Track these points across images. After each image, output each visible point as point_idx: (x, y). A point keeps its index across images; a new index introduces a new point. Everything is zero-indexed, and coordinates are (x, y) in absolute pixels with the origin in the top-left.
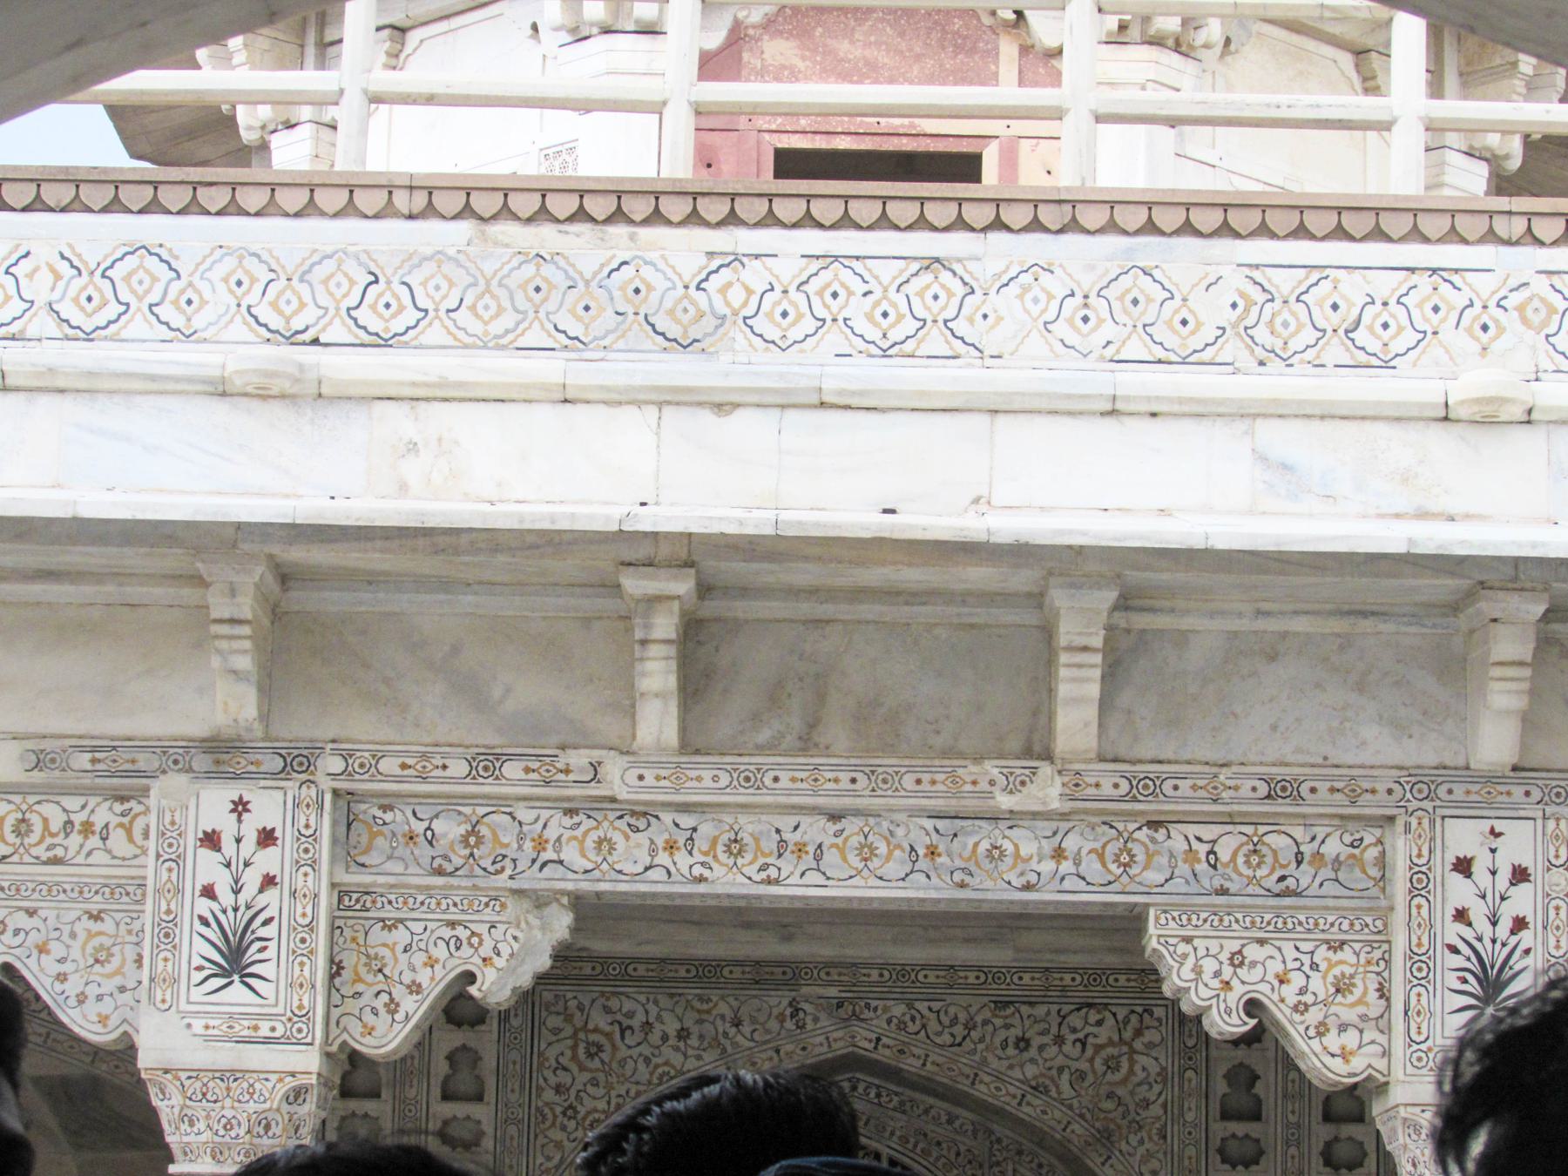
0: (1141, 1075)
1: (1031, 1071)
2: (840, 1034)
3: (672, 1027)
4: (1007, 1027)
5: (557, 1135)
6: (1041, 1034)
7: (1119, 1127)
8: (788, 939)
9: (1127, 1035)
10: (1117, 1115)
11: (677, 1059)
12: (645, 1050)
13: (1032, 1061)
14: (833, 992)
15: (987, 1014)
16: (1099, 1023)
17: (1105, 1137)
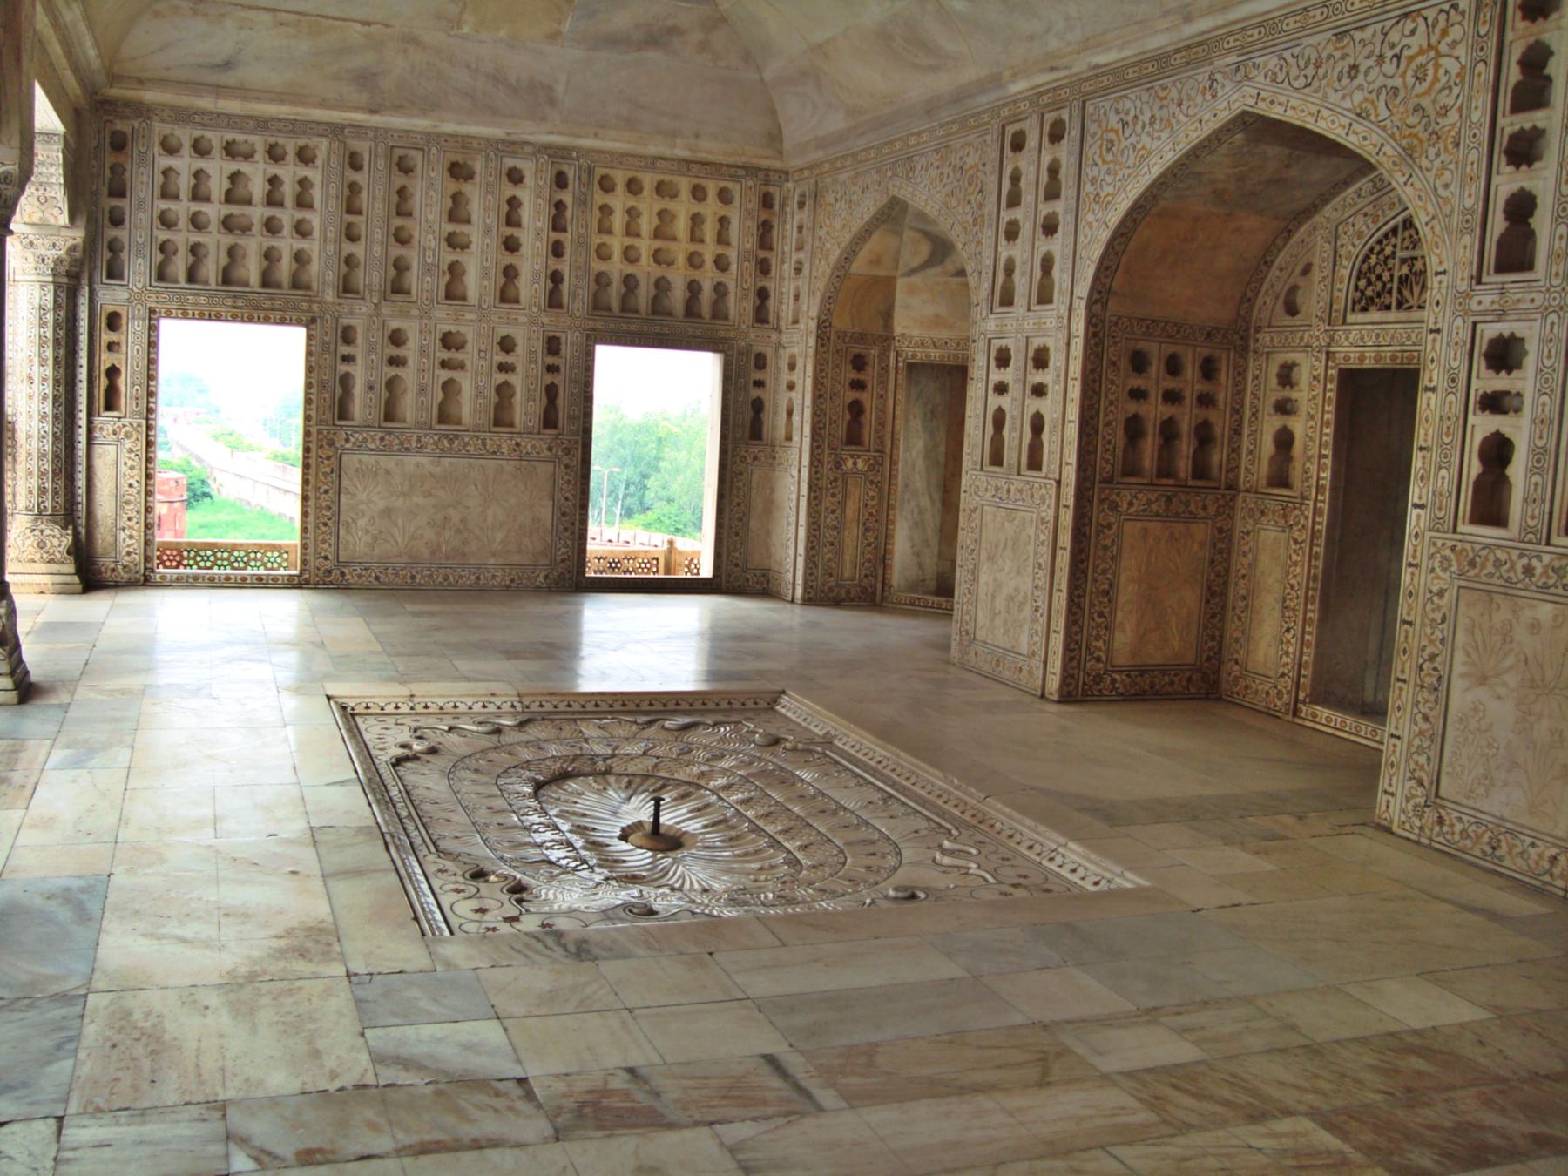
0: (1443, 80)
1: (1358, 97)
2: (1234, 97)
3: (1146, 118)
4: (1343, 57)
5: (1090, 218)
6: (1368, 57)
7: (1421, 141)
8: (1188, 19)
9: (1434, 40)
10: (1420, 128)
11: (1146, 140)
12: (1133, 139)
13: (1360, 87)
14: (1233, 59)
15: (1330, 48)
16: (1413, 32)
17: (1409, 154)
